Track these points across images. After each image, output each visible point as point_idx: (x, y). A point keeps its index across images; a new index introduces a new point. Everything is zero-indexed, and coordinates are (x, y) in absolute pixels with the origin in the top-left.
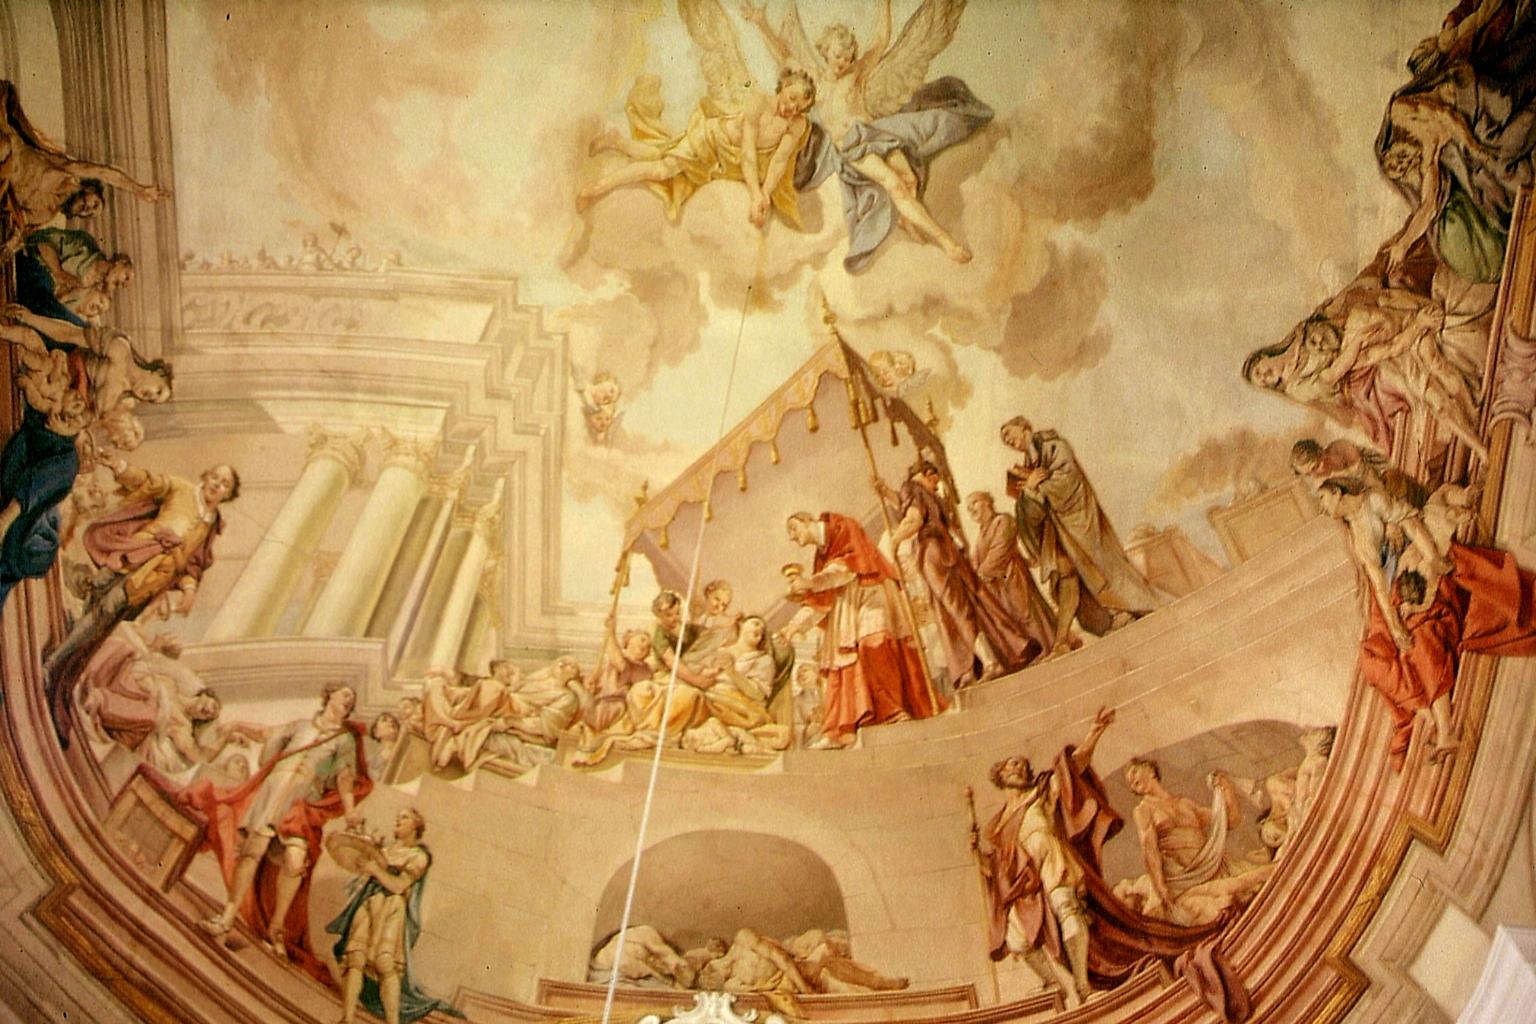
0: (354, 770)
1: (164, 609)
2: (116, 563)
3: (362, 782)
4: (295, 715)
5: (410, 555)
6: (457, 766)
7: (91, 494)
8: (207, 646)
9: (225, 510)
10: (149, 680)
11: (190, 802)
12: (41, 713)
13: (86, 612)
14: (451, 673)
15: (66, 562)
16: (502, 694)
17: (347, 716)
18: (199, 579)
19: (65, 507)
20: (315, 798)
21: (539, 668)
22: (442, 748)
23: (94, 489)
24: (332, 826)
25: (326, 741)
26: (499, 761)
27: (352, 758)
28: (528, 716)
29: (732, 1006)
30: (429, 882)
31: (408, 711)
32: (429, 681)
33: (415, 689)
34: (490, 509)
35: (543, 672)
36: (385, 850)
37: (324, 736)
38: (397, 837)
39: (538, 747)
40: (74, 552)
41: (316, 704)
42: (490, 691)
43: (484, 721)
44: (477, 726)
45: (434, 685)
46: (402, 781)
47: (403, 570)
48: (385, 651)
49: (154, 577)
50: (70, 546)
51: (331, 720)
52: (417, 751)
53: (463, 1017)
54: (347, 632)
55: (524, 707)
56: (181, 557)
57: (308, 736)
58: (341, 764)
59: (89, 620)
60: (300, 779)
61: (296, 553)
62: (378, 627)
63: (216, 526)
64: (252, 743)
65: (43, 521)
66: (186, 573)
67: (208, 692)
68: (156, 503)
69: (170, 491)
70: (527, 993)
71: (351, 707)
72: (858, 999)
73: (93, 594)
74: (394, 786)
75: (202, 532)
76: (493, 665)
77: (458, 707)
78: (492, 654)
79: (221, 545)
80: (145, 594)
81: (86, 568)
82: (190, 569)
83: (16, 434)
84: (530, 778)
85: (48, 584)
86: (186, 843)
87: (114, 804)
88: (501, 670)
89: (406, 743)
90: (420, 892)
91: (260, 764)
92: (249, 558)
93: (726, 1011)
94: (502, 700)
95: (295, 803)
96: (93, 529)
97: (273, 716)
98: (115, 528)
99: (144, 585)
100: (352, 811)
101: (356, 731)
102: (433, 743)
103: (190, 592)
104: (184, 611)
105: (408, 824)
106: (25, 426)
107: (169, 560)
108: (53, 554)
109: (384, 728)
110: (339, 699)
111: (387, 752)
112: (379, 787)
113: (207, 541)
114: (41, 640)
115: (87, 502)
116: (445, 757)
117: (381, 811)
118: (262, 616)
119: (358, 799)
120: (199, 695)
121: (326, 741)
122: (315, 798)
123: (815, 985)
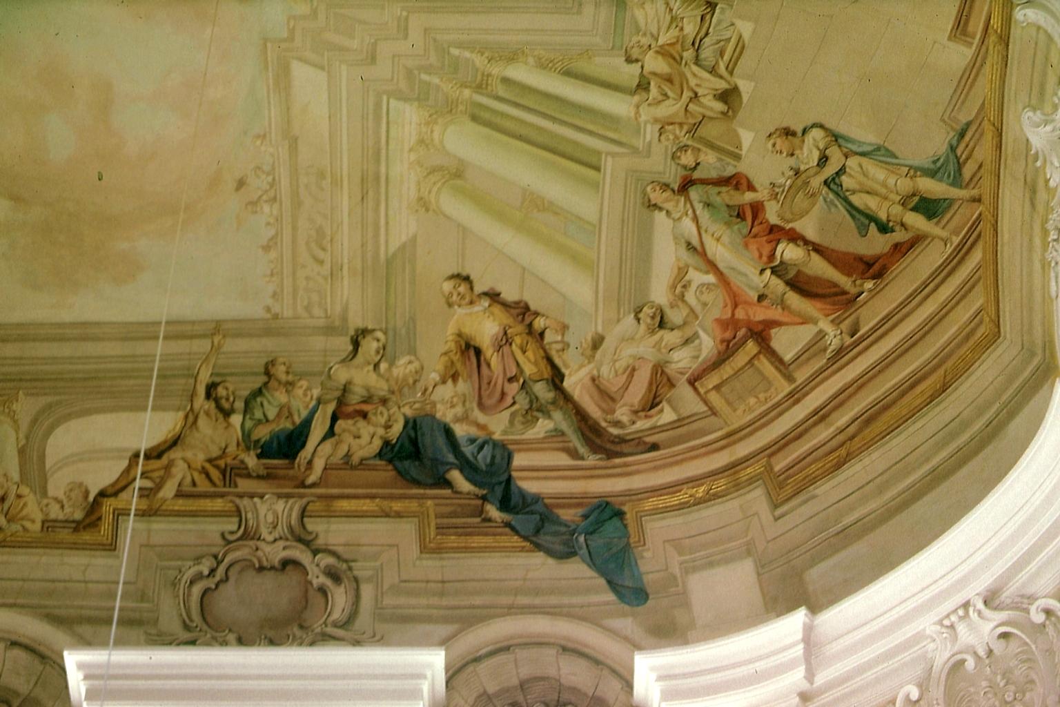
0: (724, 189)
1: (559, 346)
2: (515, 387)
3: (736, 182)
4: (668, 235)
5: (523, 131)
6: (729, 96)
7: (453, 406)
8: (596, 311)
9: (478, 289)
10: (617, 365)
11: (729, 342)
12: (626, 465)
13: (550, 417)
14: (636, 98)
15: (505, 432)
16: (657, 52)
17: (673, 191)
18: (537, 314)
19: (460, 431)
20: (745, 227)
21: (633, 17)
22: (711, 109)
23: (450, 404)
24: (772, 215)
25: (694, 211)
26: (727, 57)
27: (713, 190)
28: (682, 29)
30: (842, 129)
31: (671, 137)
32: (643, 118)
33: (651, 132)
34: (479, 61)
35: (639, 14)
36: (803, 168)
37: (690, 212)
38: (792, 155)
39: (714, 20)
40: (498, 425)
41: (660, 217)
42: (655, 64)
43: (686, 71)
44: (689, 75)
45: (646, 114)
46: (739, 147)
47: (540, 139)
48: (614, 155)
49: (530, 354)
50: (492, 427)
52: (711, 131)
54: (596, 186)
55: (674, 32)
56: (517, 329)
57: (688, 226)
58: (718, 200)
59: (558, 415)
60: (725, 239)
61: (522, 227)
62: (594, 160)
63: (494, 296)
64: (687, 278)
65: (468, 450)
66: (530, 325)
67: (638, 311)
68: (470, 349)
69: (460, 335)
71: (665, 186)
73: (536, 409)
74: (743, 153)
75: (497, 309)
76: (629, 60)
77: (670, 93)
78: (620, 61)
79: (509, 295)
80: (543, 364)
81: (513, 415)
82: (527, 321)
83: (396, 469)
84: (746, 28)
85: (520, 450)
86: (759, 352)
87: (714, 413)
88: (635, 53)
89: (702, 140)
90: (847, 139)
91: (707, 273)
92: (524, 269)
94: (663, 52)
95: (746, 246)
96: (481, 405)
97: (666, 255)
98: (484, 386)
99: (536, 364)
100: (762, 194)
101: (686, 185)
102: (704, 117)
103: (548, 323)
104: (565, 328)
105: (781, 143)
106: (390, 461)
107: (518, 340)
108: (495, 444)
109: (688, 159)
110: (656, 196)
112: (743, 167)
113: (506, 305)
114: (564, 460)
115: (459, 410)
116: (719, 106)
117: (764, 166)
118: (575, 258)
119: (751, 188)
120: (638, 320)
121: (694, 211)
122: (745, 227)
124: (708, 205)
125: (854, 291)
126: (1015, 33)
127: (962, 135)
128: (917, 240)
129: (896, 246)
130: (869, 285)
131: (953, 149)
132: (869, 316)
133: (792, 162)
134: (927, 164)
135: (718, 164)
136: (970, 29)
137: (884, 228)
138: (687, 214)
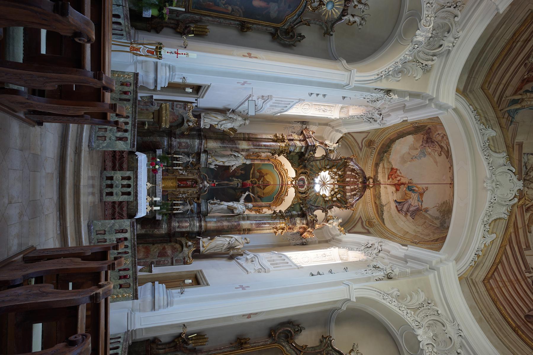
29: (520, 189)
53: (510, 125)
70: (519, 139)
72: (524, 220)
93: (518, 188)
123: (528, 210)
125: (530, 73)
126: (505, 149)
127: (511, 122)
128: (515, 93)
129: (521, 89)
130: (525, 77)
131: (513, 118)
132: (522, 69)
134: (520, 111)
136: (518, 146)
137: (527, 91)
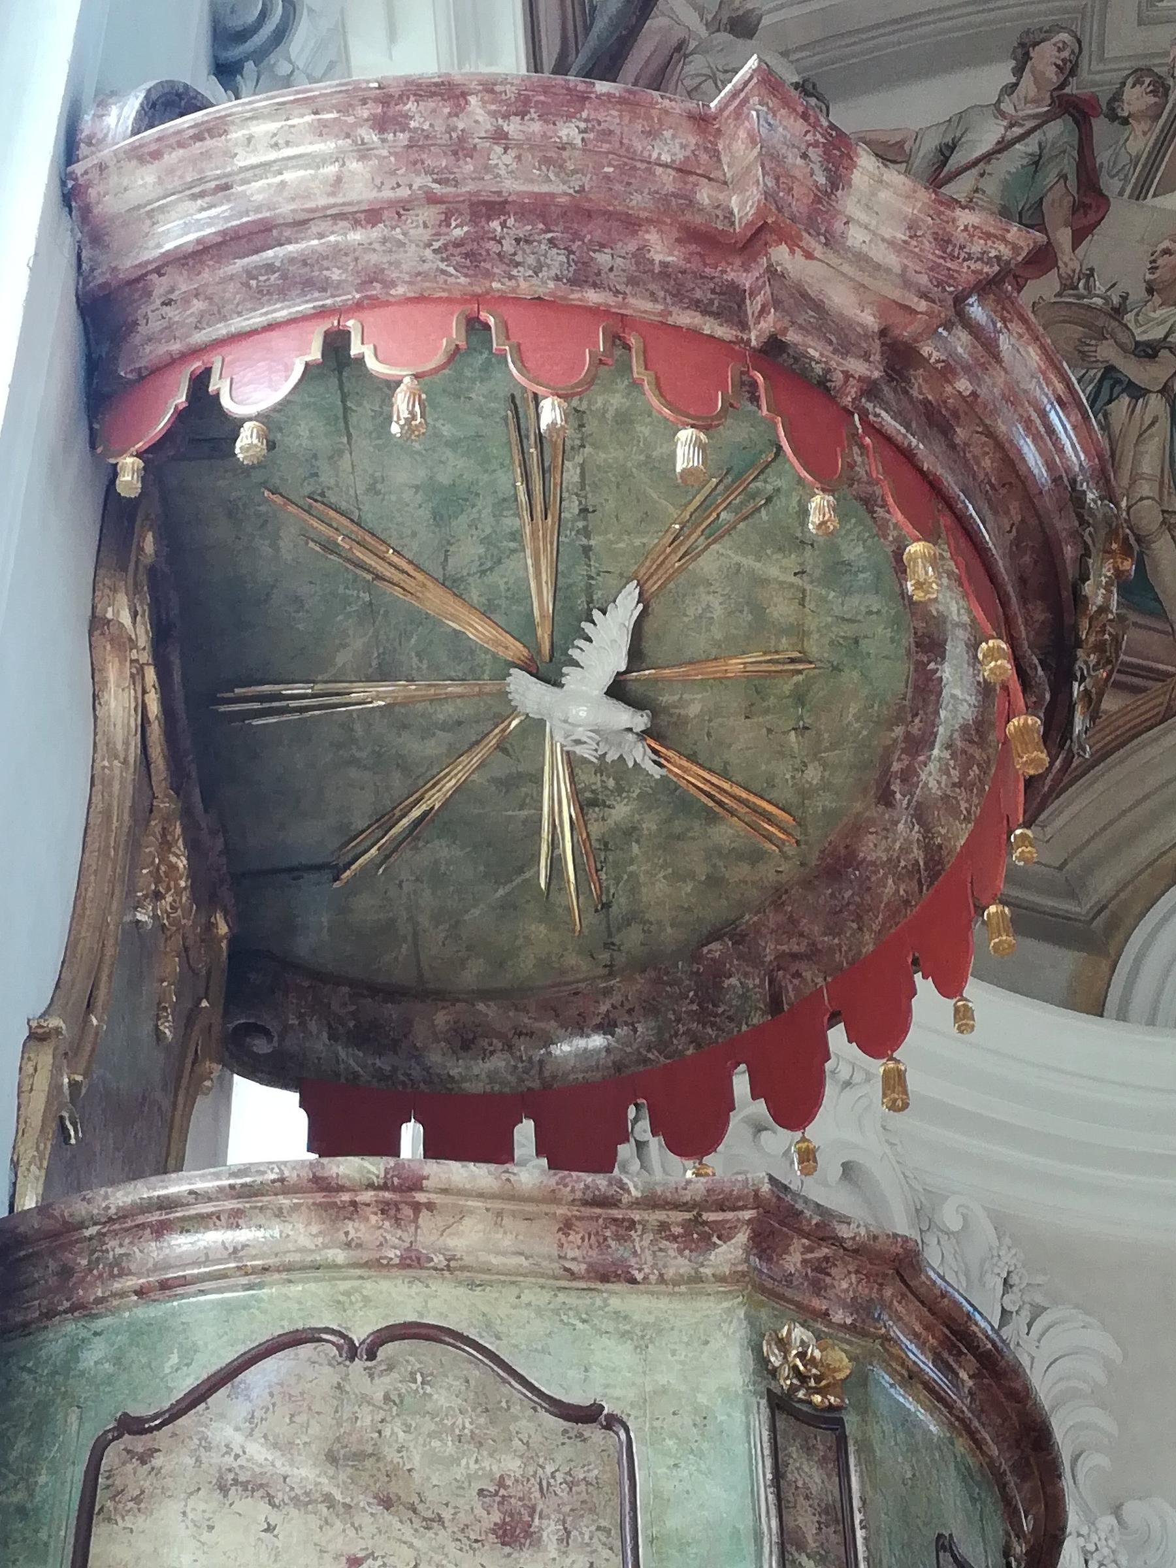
3: (1089, 205)
27: (1068, 165)
41: (1003, 73)
51: (1031, 98)
74: (1150, 201)
101: (1076, 110)
109: (1136, 99)
110: (1046, 57)
111: (1139, 141)
124: (1036, 163)
133: (1137, 293)
135: (1124, 160)
138: (1011, 126)
